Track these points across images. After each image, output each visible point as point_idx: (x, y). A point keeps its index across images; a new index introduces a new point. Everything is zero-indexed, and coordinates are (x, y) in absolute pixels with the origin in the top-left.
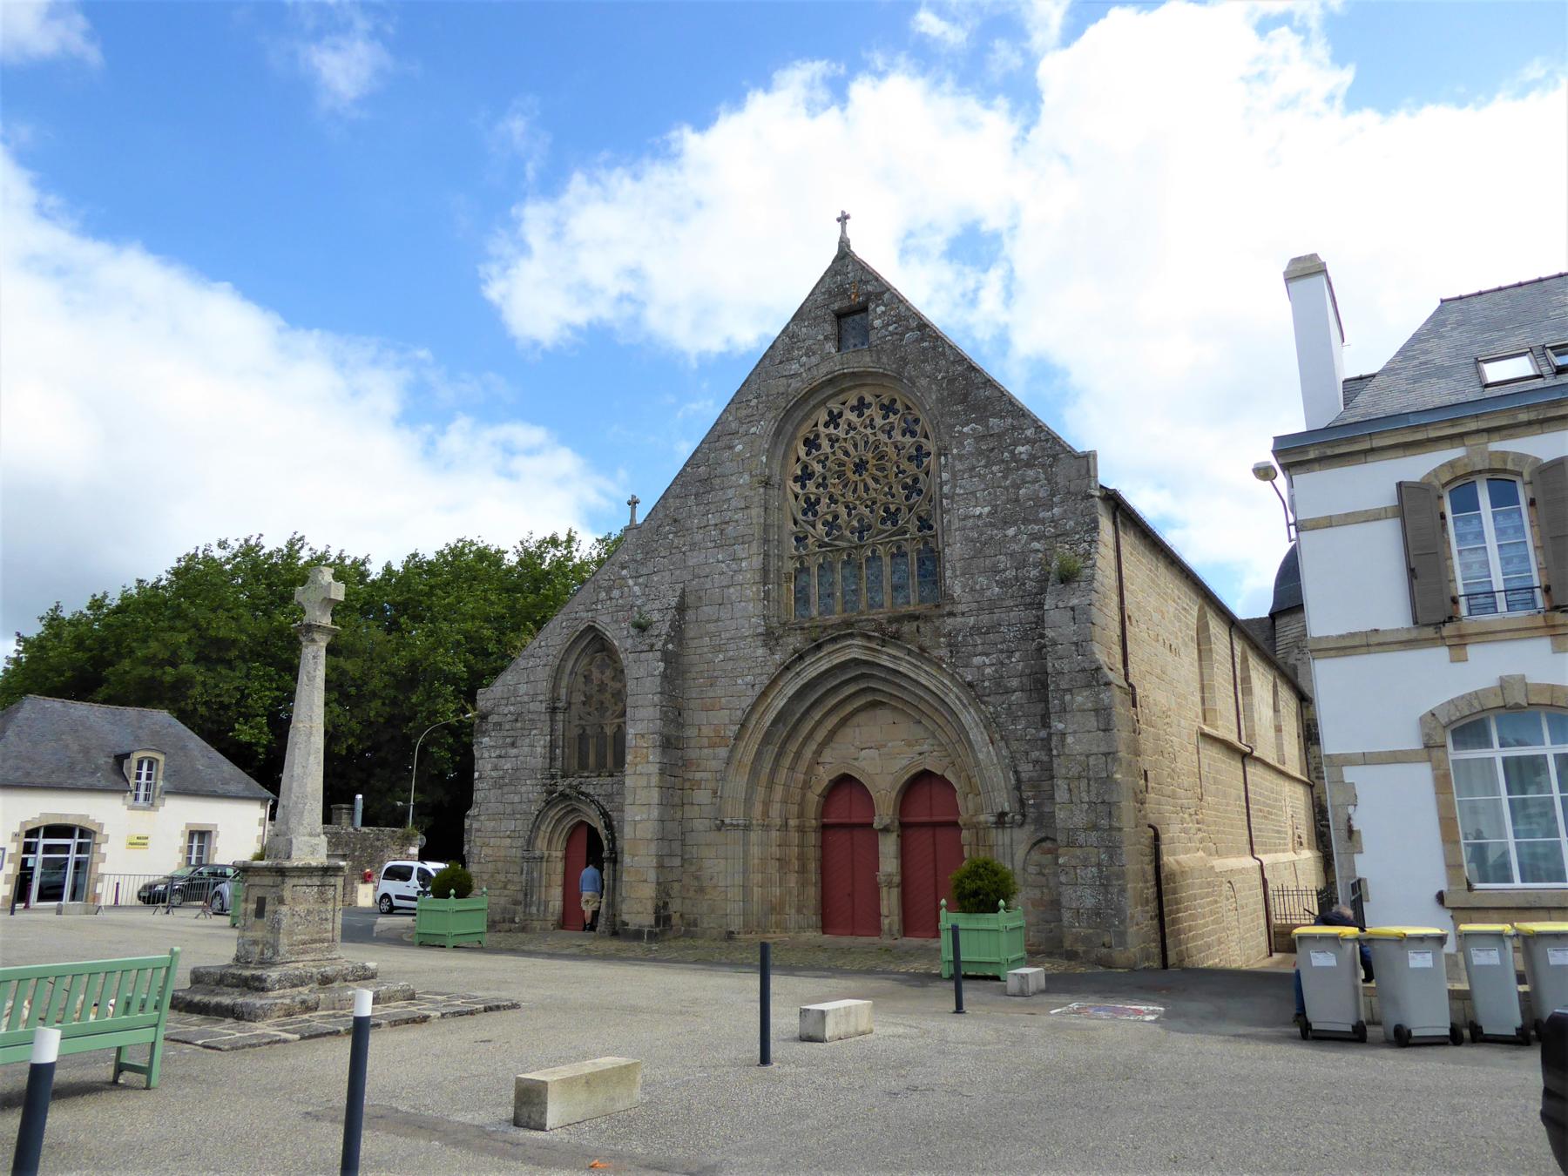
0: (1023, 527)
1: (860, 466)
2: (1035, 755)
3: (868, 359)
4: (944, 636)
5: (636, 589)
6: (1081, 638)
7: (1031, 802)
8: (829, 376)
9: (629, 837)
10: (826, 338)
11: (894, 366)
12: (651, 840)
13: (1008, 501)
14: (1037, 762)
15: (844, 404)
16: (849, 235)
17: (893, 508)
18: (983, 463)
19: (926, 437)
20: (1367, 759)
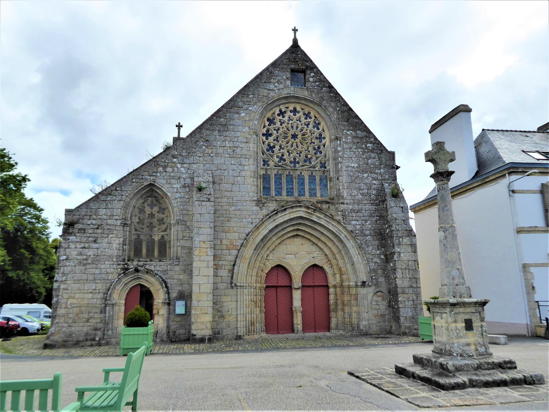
0: (370, 174)
1: (294, 136)
2: (375, 260)
3: (306, 93)
4: (340, 211)
5: (182, 169)
6: (406, 219)
7: (374, 277)
8: (288, 95)
9: (196, 292)
10: (287, 78)
11: (318, 99)
12: (210, 293)
13: (364, 164)
14: (376, 263)
15: (287, 108)
16: (297, 37)
18: (355, 147)
19: (323, 131)
20: (537, 265)
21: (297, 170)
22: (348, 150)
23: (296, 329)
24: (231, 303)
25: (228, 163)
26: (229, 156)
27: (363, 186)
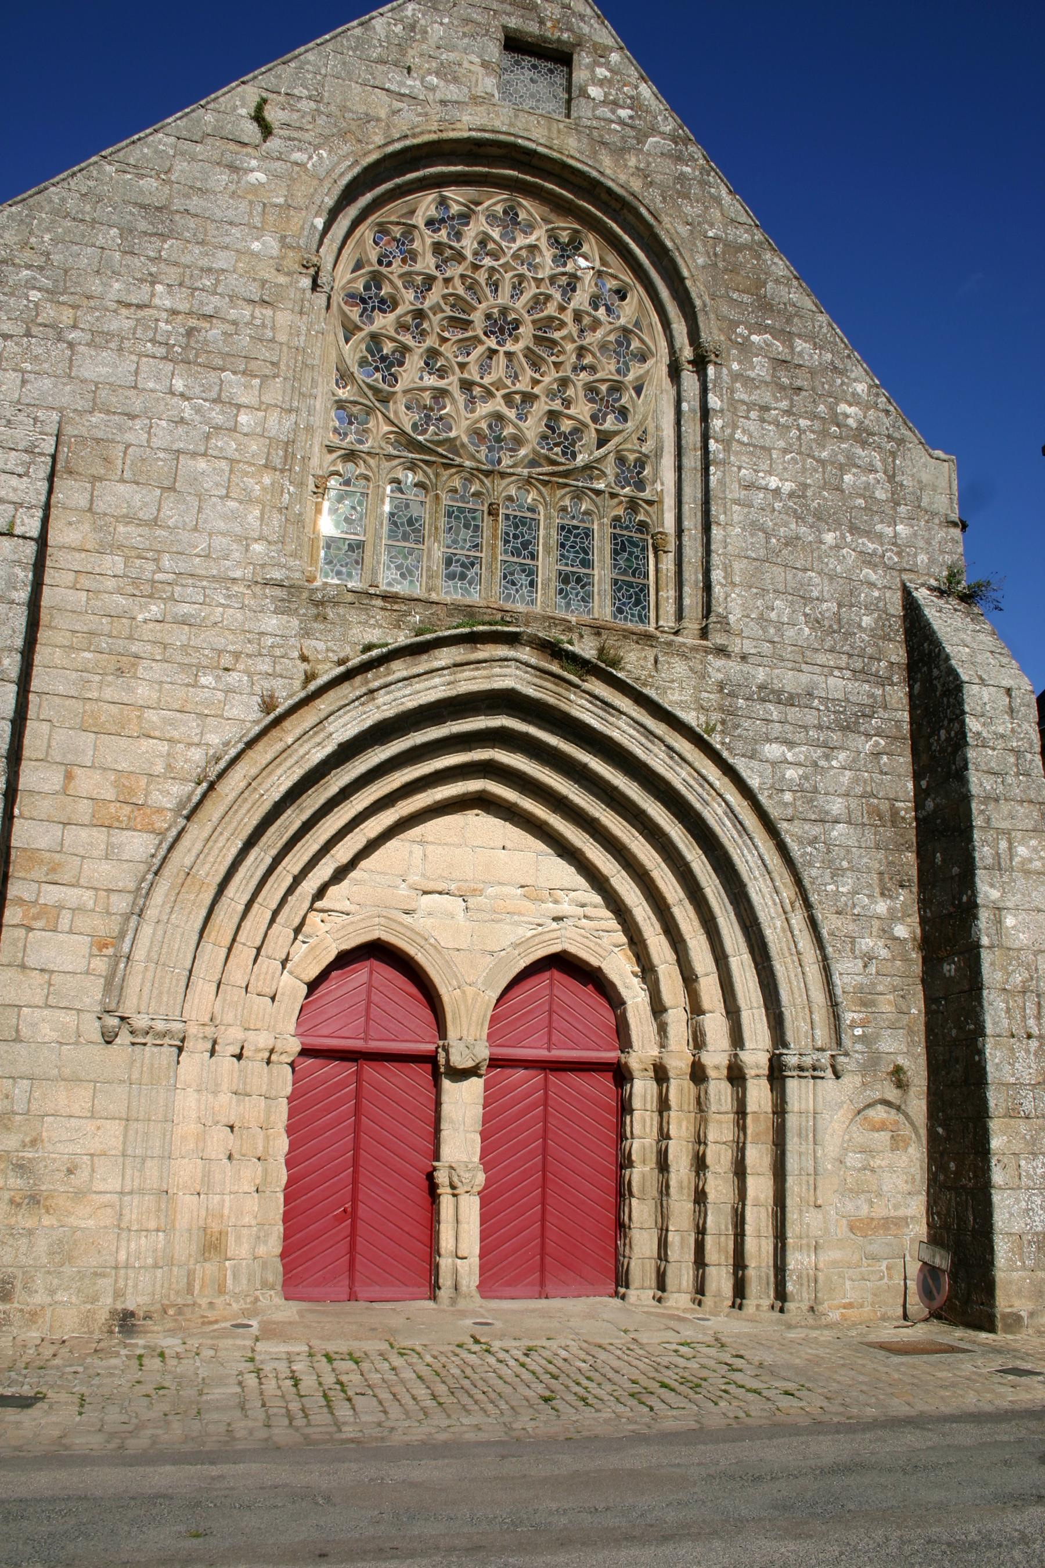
0: (849, 539)
2: (866, 943)
7: (858, 1032)
17: (566, 425)
18: (784, 404)
21: (503, 475)
22: (753, 415)
23: (446, 1280)
24: (90, 1126)
25: (151, 385)
26: (161, 351)
27: (818, 585)
